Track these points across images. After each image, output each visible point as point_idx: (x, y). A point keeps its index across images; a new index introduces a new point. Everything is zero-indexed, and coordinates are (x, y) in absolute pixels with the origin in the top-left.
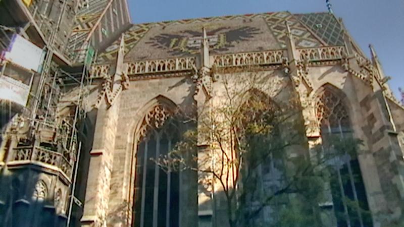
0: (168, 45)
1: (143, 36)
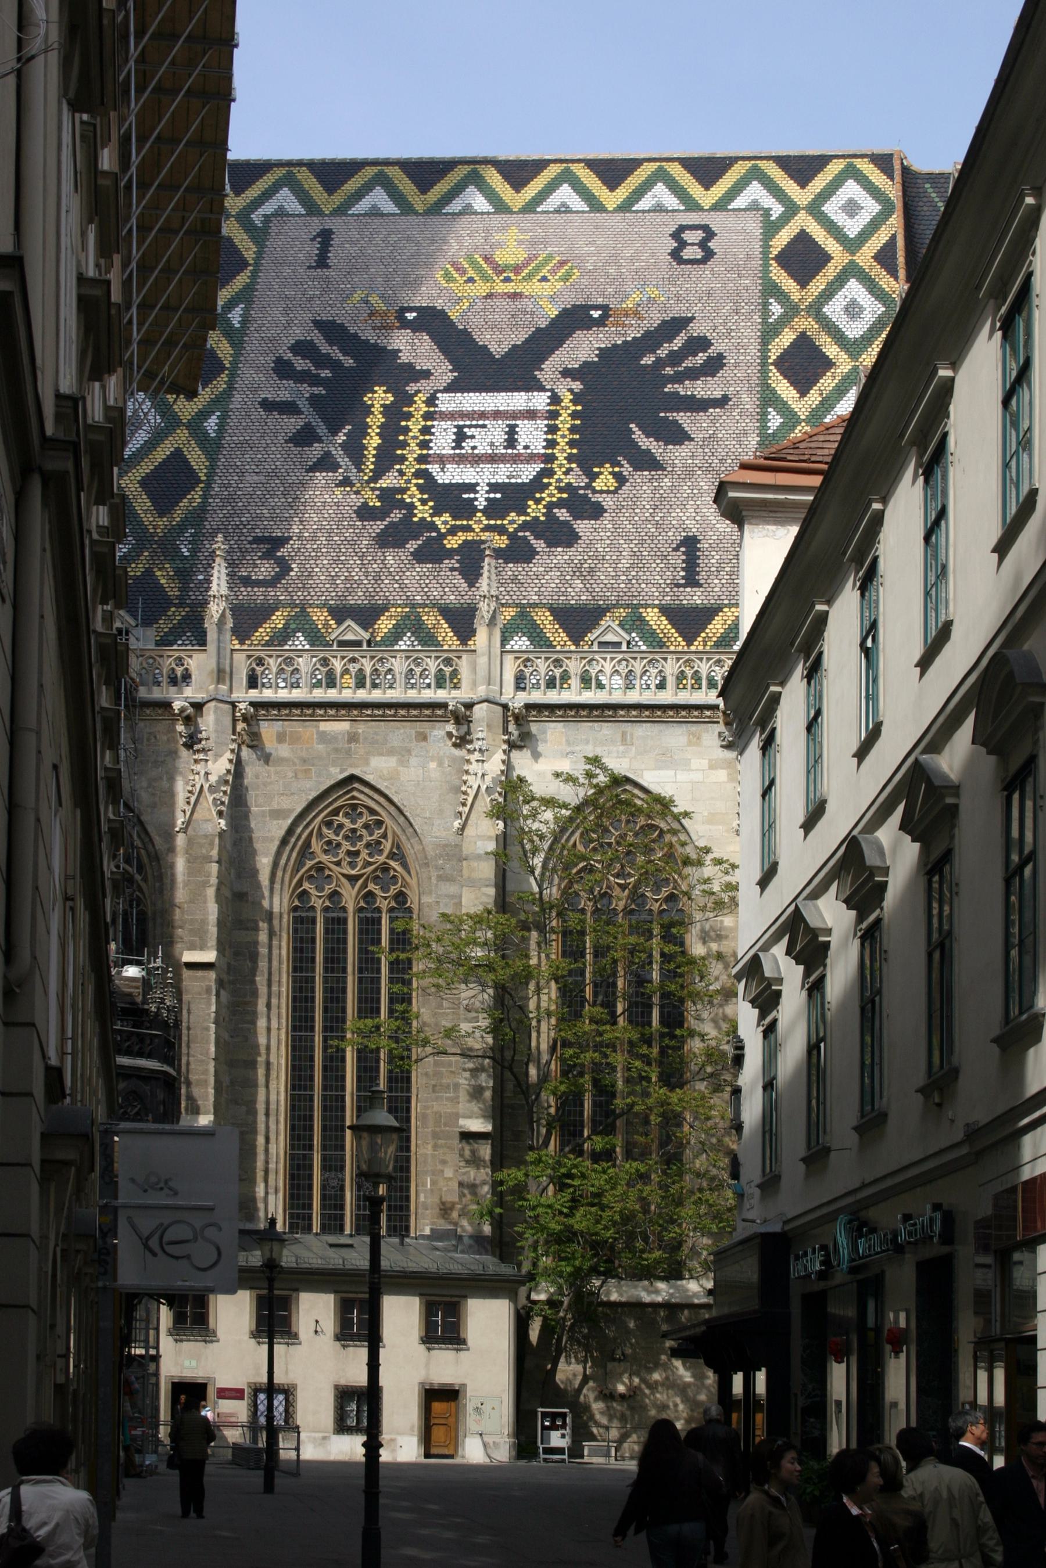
0: (355, 450)
1: (245, 321)
